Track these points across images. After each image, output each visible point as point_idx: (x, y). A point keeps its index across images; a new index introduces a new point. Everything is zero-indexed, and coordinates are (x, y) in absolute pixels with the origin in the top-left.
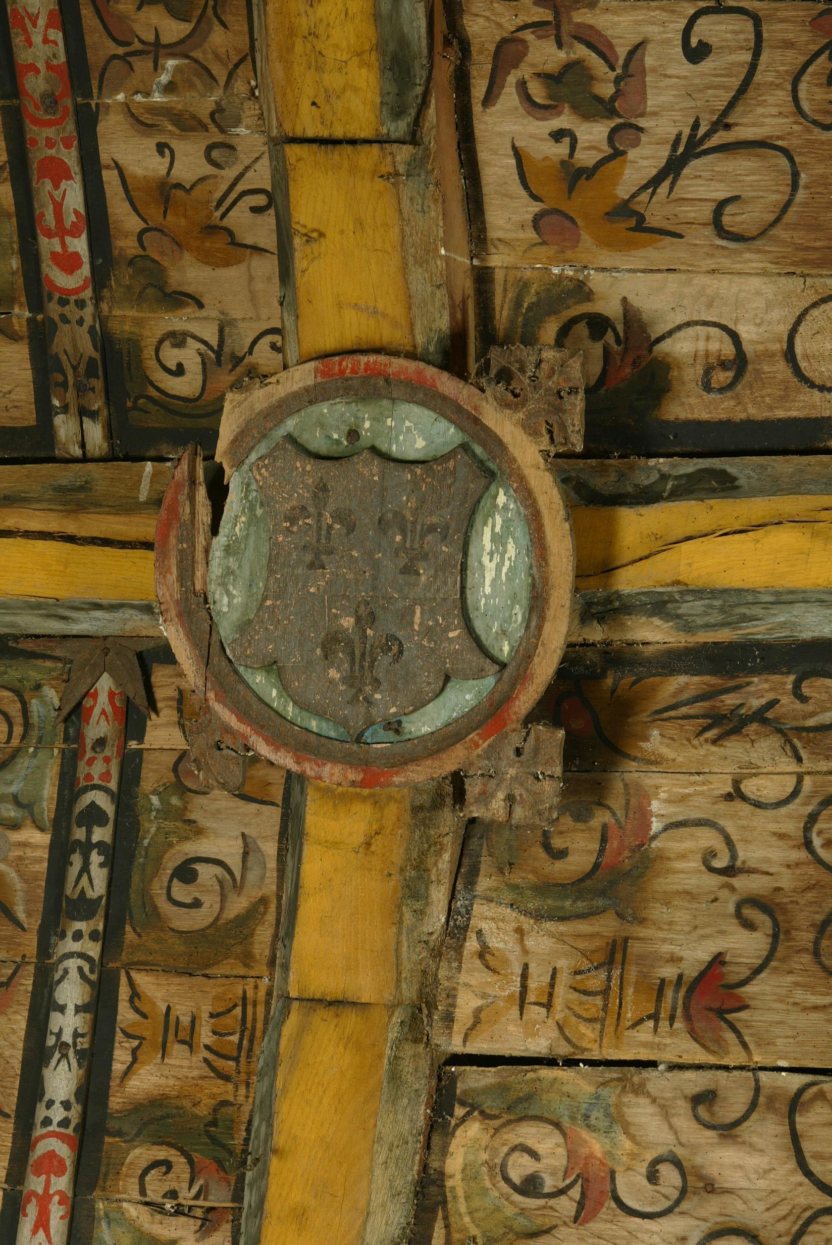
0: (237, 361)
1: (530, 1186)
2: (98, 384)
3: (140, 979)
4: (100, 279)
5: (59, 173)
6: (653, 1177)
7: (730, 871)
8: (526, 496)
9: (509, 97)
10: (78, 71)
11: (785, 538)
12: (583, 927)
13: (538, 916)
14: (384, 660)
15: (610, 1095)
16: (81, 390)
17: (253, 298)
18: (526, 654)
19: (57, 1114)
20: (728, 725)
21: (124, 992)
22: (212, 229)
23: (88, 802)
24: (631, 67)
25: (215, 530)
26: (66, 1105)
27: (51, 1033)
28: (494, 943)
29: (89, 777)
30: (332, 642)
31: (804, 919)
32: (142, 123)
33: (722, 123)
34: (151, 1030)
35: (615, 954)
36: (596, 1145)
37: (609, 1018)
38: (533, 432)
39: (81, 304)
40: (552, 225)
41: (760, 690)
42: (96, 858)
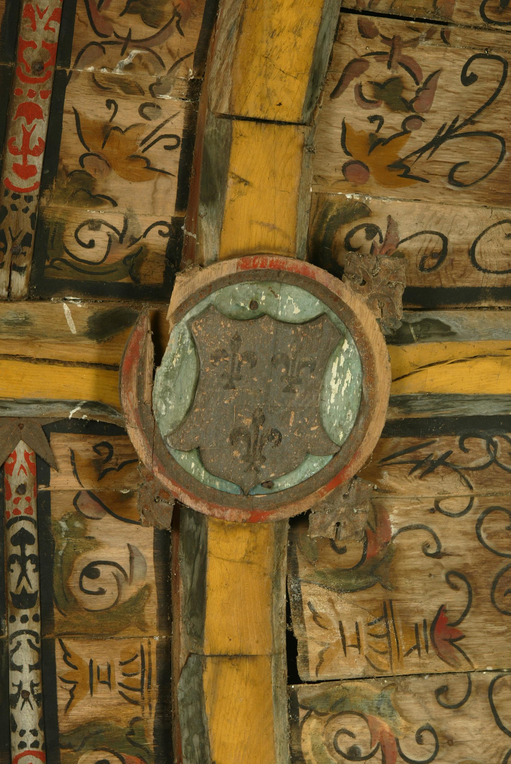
0: (134, 240)
1: (353, 754)
2: (29, 250)
3: (70, 644)
4: (45, 184)
5: (32, 113)
6: (419, 740)
7: (438, 555)
8: (363, 345)
9: (349, 93)
10: (64, 49)
11: (486, 365)
12: (365, 595)
13: (340, 591)
14: (268, 446)
15: (390, 694)
16: (15, 254)
17: (154, 202)
18: (355, 439)
19: (29, 739)
20: (427, 468)
21: (59, 653)
22: (134, 158)
23: (19, 528)
24: (428, 85)
25: (158, 361)
26: (34, 732)
27: (14, 685)
28: (320, 610)
29: (16, 511)
30: (236, 435)
31: (484, 581)
32: (98, 85)
33: (470, 121)
34: (82, 677)
35: (386, 611)
36: (386, 725)
37: (393, 652)
38: (371, 307)
39: (29, 199)
40: (355, 171)
41: (440, 445)
42: (30, 566)
